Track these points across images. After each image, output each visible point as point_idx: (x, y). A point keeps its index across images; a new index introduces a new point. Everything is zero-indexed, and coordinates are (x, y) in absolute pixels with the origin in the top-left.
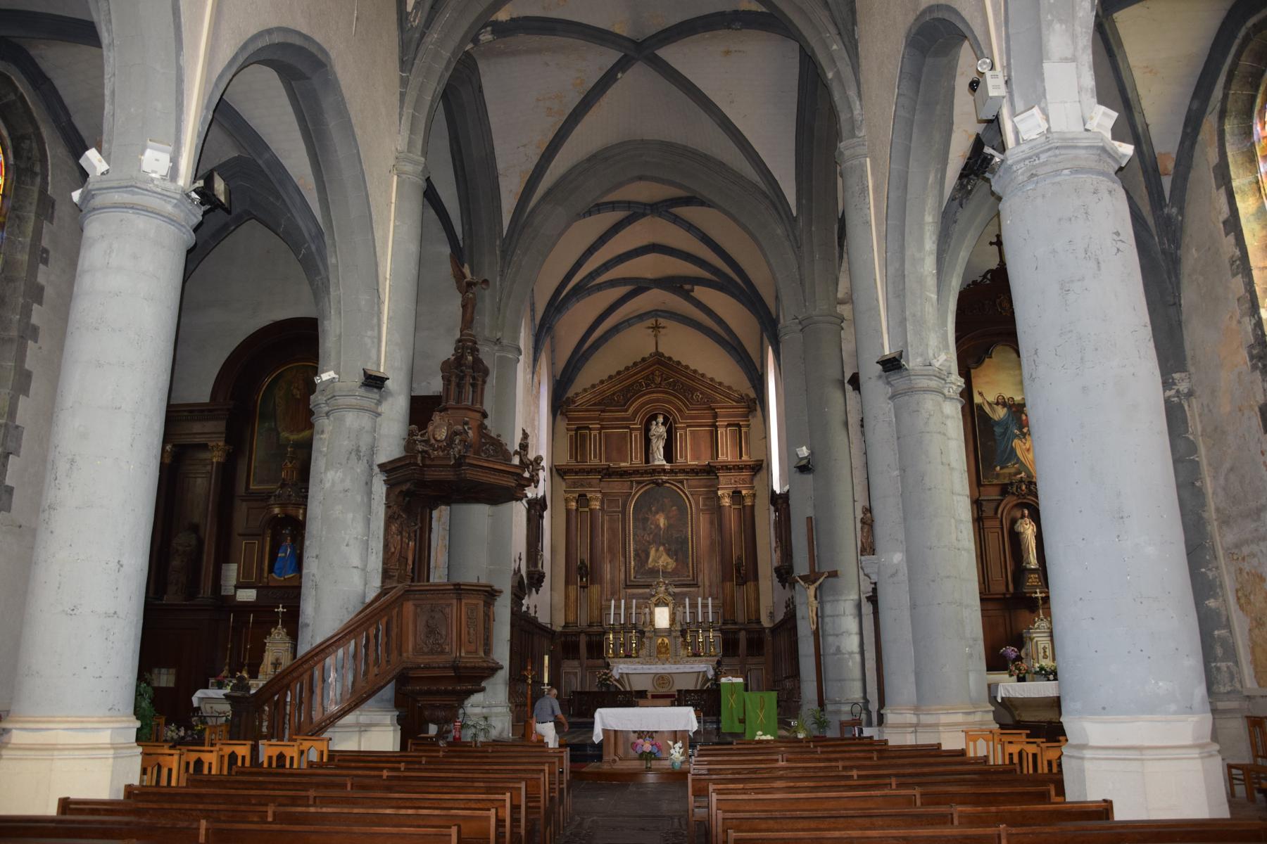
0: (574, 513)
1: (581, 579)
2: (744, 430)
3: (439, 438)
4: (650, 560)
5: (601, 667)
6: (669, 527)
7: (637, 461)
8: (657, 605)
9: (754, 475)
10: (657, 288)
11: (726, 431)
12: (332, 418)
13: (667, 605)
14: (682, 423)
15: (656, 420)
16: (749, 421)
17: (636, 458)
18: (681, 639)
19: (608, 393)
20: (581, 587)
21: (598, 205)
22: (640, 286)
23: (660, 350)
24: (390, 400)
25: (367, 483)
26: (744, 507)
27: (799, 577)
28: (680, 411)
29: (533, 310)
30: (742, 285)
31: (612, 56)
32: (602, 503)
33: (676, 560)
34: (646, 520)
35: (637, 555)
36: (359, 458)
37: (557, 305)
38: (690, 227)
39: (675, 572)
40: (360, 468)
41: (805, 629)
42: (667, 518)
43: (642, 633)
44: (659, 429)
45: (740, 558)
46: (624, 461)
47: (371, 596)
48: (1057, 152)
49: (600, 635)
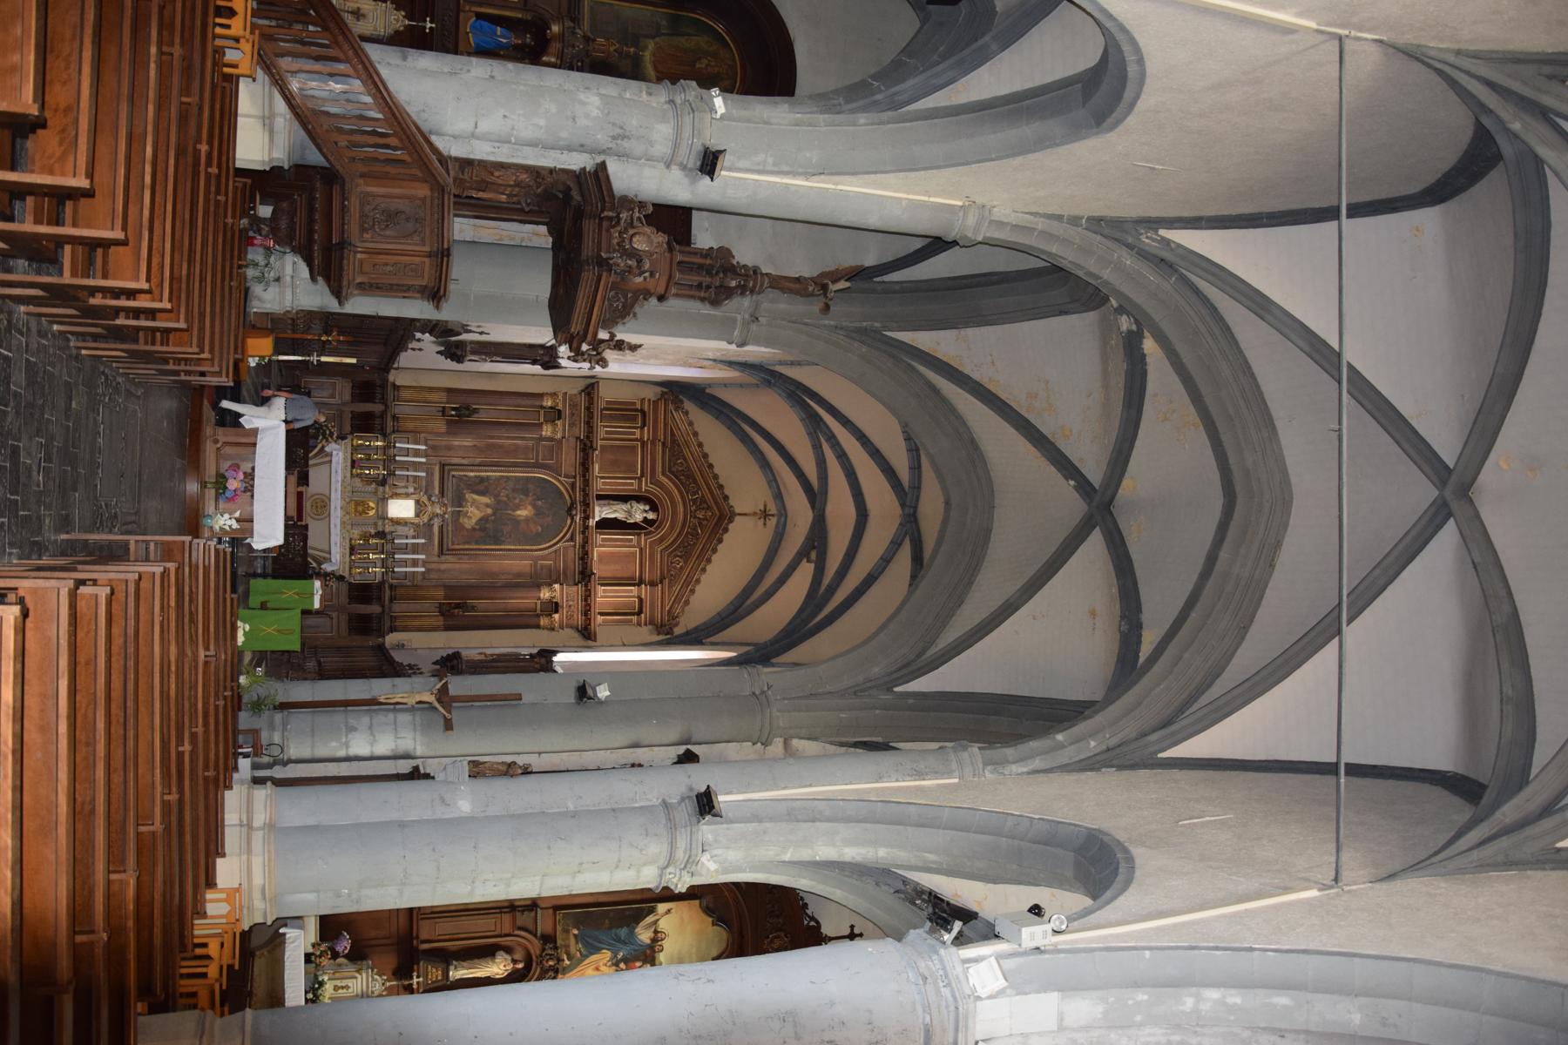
0: (538, 403)
1: (454, 409)
2: (635, 618)
3: (634, 240)
5: (340, 429)
7: (600, 485)
8: (417, 502)
9: (577, 629)
10: (814, 517)
11: (634, 597)
12: (666, 106)
13: (417, 515)
14: (646, 541)
15: (651, 509)
16: (646, 625)
17: (604, 484)
18: (373, 531)
19: (686, 452)
20: (444, 408)
21: (917, 450)
22: (816, 497)
23: (737, 519)
24: (686, 181)
25: (582, 146)
26: (538, 616)
27: (446, 682)
28: (661, 540)
29: (792, 363)
30: (814, 622)
31: (1095, 475)
32: (551, 439)
33: (474, 529)
34: (526, 492)
35: (482, 480)
36: (614, 138)
37: (798, 394)
38: (886, 560)
39: (458, 527)
40: (602, 139)
41: (379, 688)
42: (527, 520)
43: (383, 483)
44: (638, 513)
45: (473, 608)
46: (601, 470)
47: (438, 142)
48: (952, 1008)
49: (382, 429)
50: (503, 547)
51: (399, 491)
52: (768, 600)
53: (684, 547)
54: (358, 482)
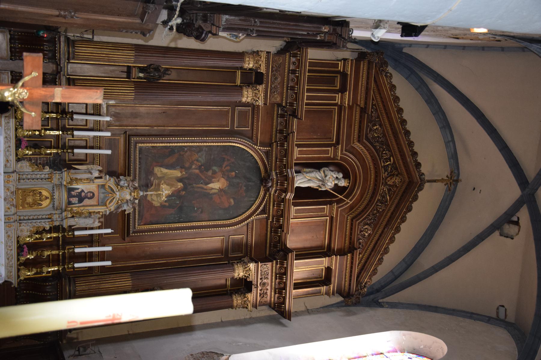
2: (324, 289)
4: (165, 171)
6: (207, 196)
15: (344, 177)
18: (47, 228)
23: (427, 185)
28: (351, 208)
32: (247, 105)
33: (162, 206)
35: (172, 151)
50: (194, 224)
51: (79, 176)
52: (448, 265)
53: (373, 214)
54: (25, 167)
